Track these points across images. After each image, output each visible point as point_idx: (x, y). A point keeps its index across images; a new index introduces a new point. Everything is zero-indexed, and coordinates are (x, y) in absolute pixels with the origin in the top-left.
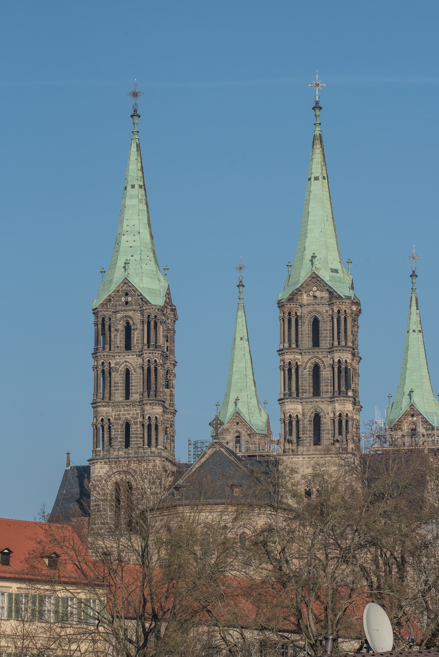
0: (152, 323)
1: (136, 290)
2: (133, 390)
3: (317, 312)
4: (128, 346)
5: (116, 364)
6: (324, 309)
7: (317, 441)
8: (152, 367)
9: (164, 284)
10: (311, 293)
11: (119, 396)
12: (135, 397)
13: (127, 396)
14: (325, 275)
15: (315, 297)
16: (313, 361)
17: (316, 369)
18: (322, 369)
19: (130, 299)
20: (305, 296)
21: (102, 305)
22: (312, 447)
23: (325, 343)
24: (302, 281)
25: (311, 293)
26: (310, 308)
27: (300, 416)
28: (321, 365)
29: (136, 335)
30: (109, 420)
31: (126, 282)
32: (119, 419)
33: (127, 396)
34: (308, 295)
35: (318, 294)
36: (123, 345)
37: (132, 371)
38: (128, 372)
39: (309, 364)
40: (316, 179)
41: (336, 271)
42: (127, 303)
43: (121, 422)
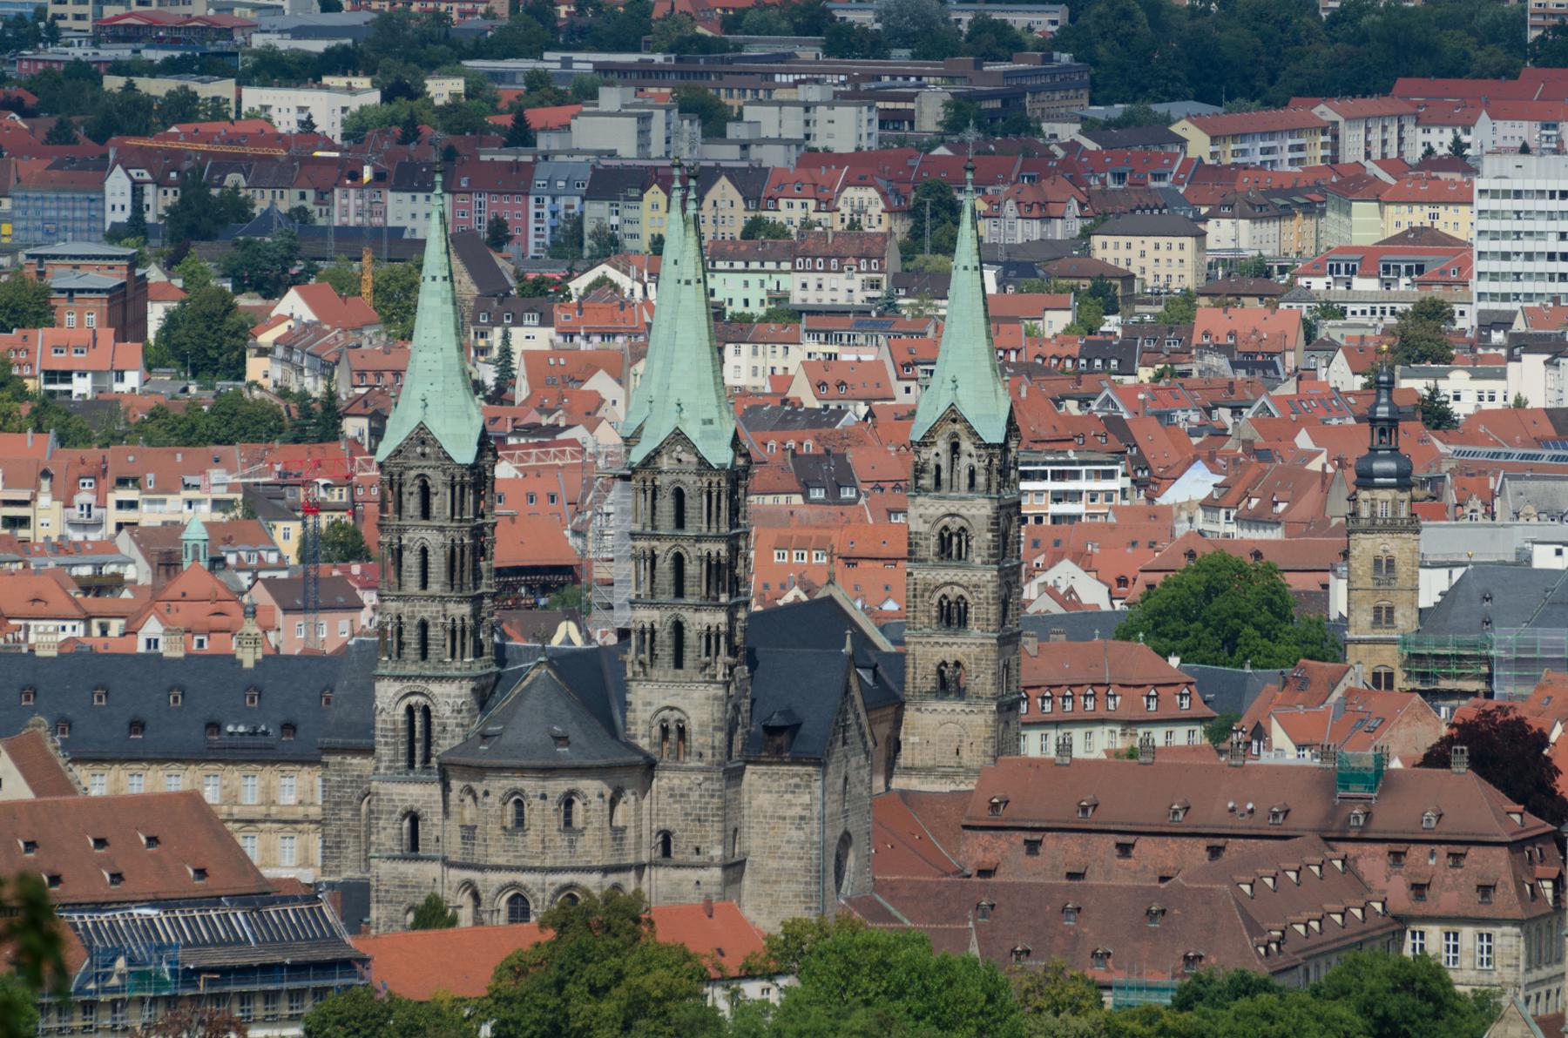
0: (457, 488)
1: (436, 441)
2: (432, 578)
4: (426, 513)
5: (410, 540)
6: (690, 480)
7: (678, 663)
8: (458, 550)
9: (478, 422)
11: (412, 585)
12: (435, 588)
13: (424, 584)
14: (693, 431)
15: (680, 461)
16: (674, 550)
17: (679, 560)
18: (687, 561)
19: (427, 450)
20: (665, 459)
21: (389, 457)
22: (671, 672)
23: (690, 531)
24: (662, 437)
26: (674, 477)
27: (657, 626)
29: (435, 502)
30: (399, 618)
31: (422, 427)
32: (413, 617)
33: (424, 584)
34: (671, 457)
35: (684, 456)
36: (418, 513)
37: (430, 550)
38: (424, 551)
39: (671, 555)
40: (688, 283)
41: (710, 422)
42: (423, 455)
43: (416, 622)
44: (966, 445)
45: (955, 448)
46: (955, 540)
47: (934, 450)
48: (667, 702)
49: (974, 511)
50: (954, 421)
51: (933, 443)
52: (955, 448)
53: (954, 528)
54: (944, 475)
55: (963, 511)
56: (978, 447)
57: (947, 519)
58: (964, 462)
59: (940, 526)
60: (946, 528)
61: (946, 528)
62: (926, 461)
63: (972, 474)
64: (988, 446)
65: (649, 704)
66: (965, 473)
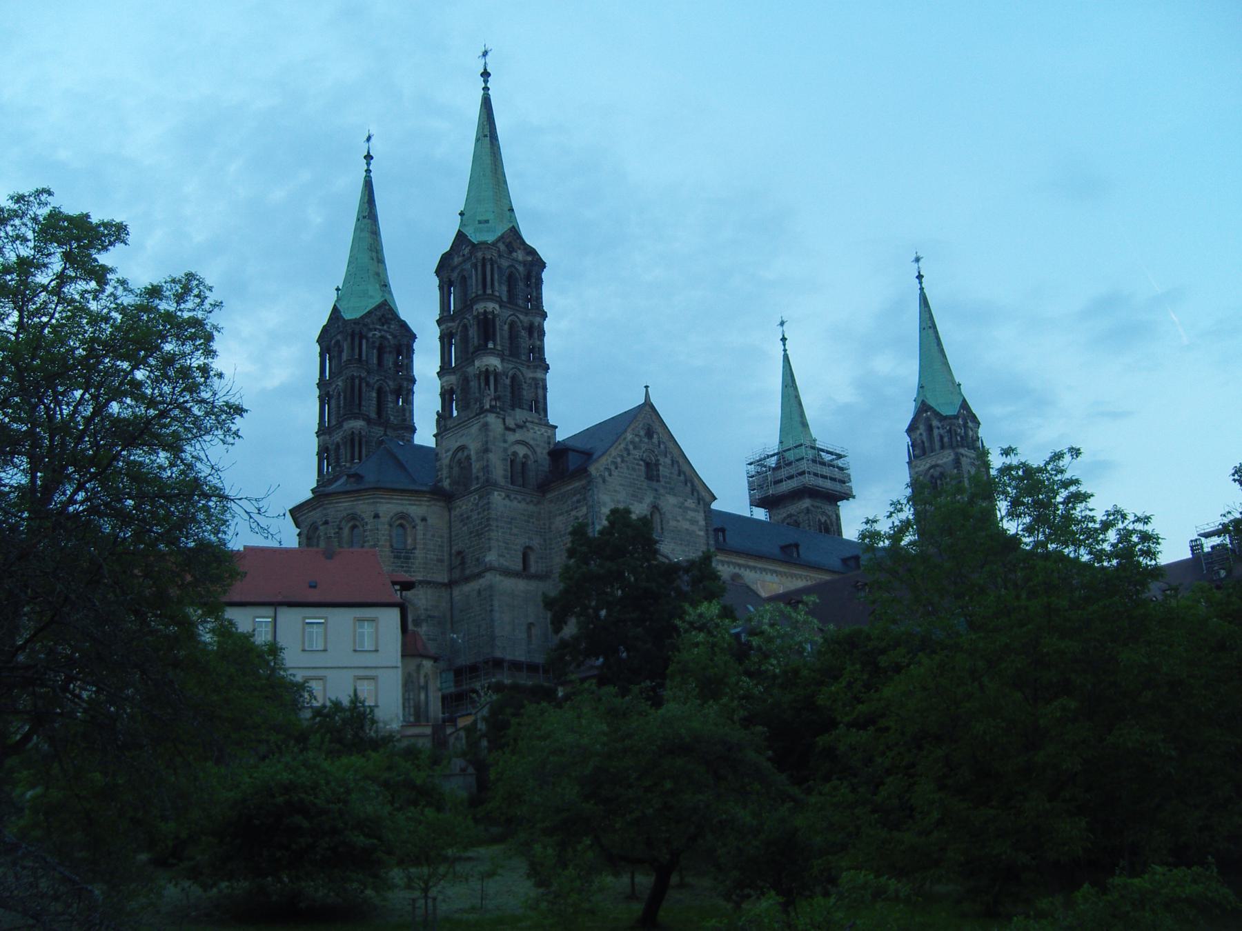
3: (465, 270)
10: (461, 254)
15: (464, 255)
25: (461, 254)
28: (468, 324)
34: (459, 256)
44: (935, 423)
45: (930, 429)
46: (939, 482)
47: (918, 432)
48: (458, 444)
49: (945, 460)
50: (926, 412)
51: (918, 428)
52: (930, 429)
53: (937, 474)
54: (926, 444)
55: (940, 462)
56: (940, 421)
57: (932, 470)
58: (936, 432)
59: (928, 476)
60: (932, 476)
61: (932, 476)
62: (915, 440)
63: (941, 437)
64: (946, 418)
65: (447, 451)
66: (937, 438)
